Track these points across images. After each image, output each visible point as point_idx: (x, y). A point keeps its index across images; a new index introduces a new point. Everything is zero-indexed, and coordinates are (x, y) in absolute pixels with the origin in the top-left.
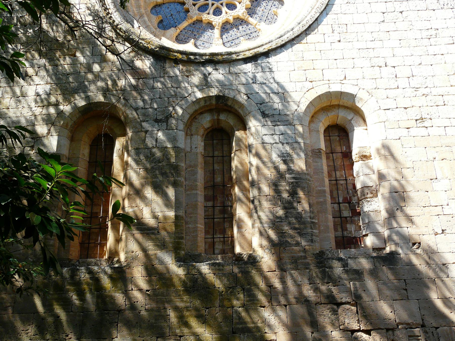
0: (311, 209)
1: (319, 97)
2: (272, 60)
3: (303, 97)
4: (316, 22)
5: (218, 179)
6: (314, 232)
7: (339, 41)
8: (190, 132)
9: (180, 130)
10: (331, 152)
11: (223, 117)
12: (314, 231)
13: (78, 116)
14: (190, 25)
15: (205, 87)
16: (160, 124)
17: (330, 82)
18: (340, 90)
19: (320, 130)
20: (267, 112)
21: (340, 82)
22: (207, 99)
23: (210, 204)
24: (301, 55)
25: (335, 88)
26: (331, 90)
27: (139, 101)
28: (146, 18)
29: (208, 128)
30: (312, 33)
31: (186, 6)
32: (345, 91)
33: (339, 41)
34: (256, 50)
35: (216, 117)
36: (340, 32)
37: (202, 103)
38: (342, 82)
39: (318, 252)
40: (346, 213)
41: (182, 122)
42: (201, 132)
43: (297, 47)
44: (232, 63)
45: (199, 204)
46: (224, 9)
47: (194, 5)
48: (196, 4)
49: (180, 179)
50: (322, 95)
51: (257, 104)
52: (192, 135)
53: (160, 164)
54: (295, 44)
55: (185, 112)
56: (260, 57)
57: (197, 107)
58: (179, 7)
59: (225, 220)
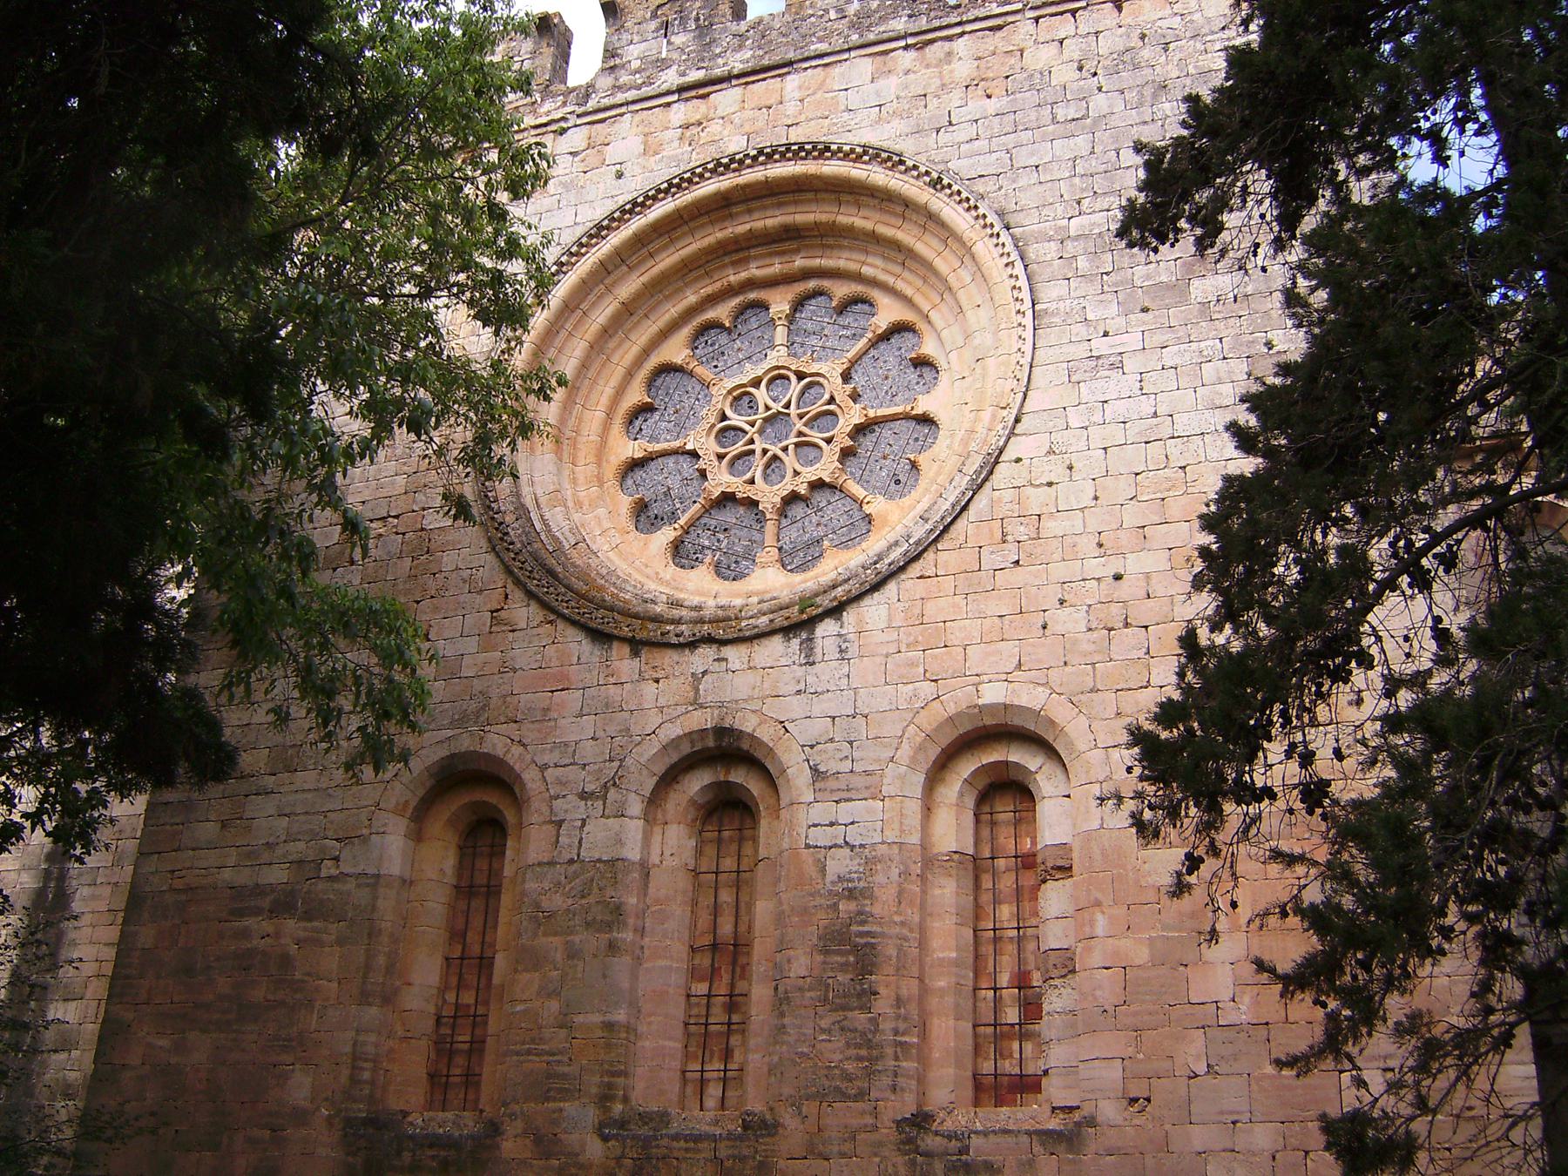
3: (911, 722)
4: (965, 514)
5: (726, 928)
7: (1017, 562)
8: (664, 816)
10: (976, 866)
11: (738, 776)
13: (428, 785)
14: (707, 511)
15: (690, 708)
16: (589, 803)
18: (1001, 701)
20: (822, 768)
21: (1004, 677)
22: (695, 736)
23: (701, 988)
24: (917, 611)
31: (701, 464)
36: (1021, 539)
40: (1012, 1015)
41: (638, 798)
44: (755, 641)
46: (790, 460)
47: (721, 457)
48: (727, 454)
49: (625, 936)
51: (803, 746)
53: (583, 901)
58: (685, 464)
59: (733, 1027)
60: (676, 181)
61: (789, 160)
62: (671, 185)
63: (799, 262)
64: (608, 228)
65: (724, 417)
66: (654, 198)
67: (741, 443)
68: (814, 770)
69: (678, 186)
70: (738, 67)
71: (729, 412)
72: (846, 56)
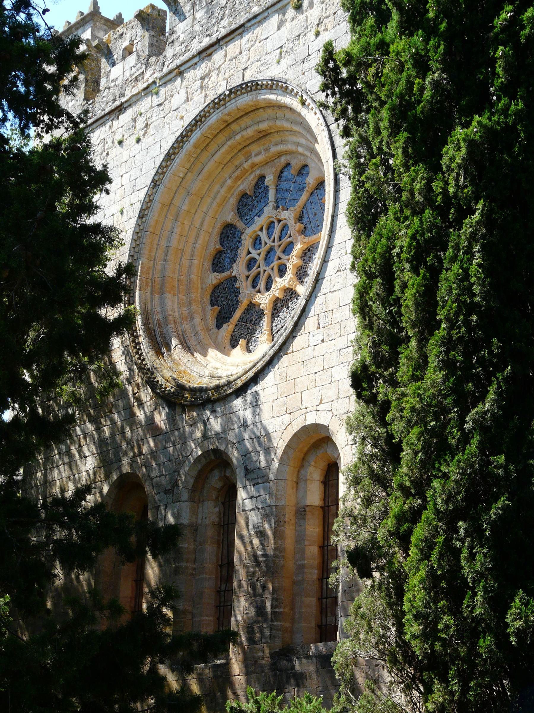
0: (275, 595)
1: (295, 435)
2: (258, 388)
6: (275, 625)
7: (323, 341)
9: (184, 502)
12: (275, 623)
17: (308, 410)
19: (308, 477)
20: (249, 467)
21: (315, 408)
24: (285, 374)
25: (311, 420)
26: (307, 423)
27: (165, 460)
28: (197, 320)
29: (222, 487)
30: (299, 334)
32: (319, 423)
33: (323, 341)
34: (244, 378)
35: (223, 473)
37: (203, 461)
38: (318, 408)
39: (277, 650)
41: (186, 490)
42: (214, 494)
43: (285, 360)
45: (206, 590)
50: (298, 431)
52: (203, 501)
54: (281, 357)
55: (188, 476)
56: (250, 384)
57: (199, 467)
60: (198, 118)
61: (245, 93)
62: (197, 122)
63: (274, 149)
64: (174, 154)
65: (249, 253)
66: (192, 131)
67: (255, 268)
68: (246, 468)
69: (201, 121)
70: (224, 32)
71: (251, 250)
72: (266, 14)
